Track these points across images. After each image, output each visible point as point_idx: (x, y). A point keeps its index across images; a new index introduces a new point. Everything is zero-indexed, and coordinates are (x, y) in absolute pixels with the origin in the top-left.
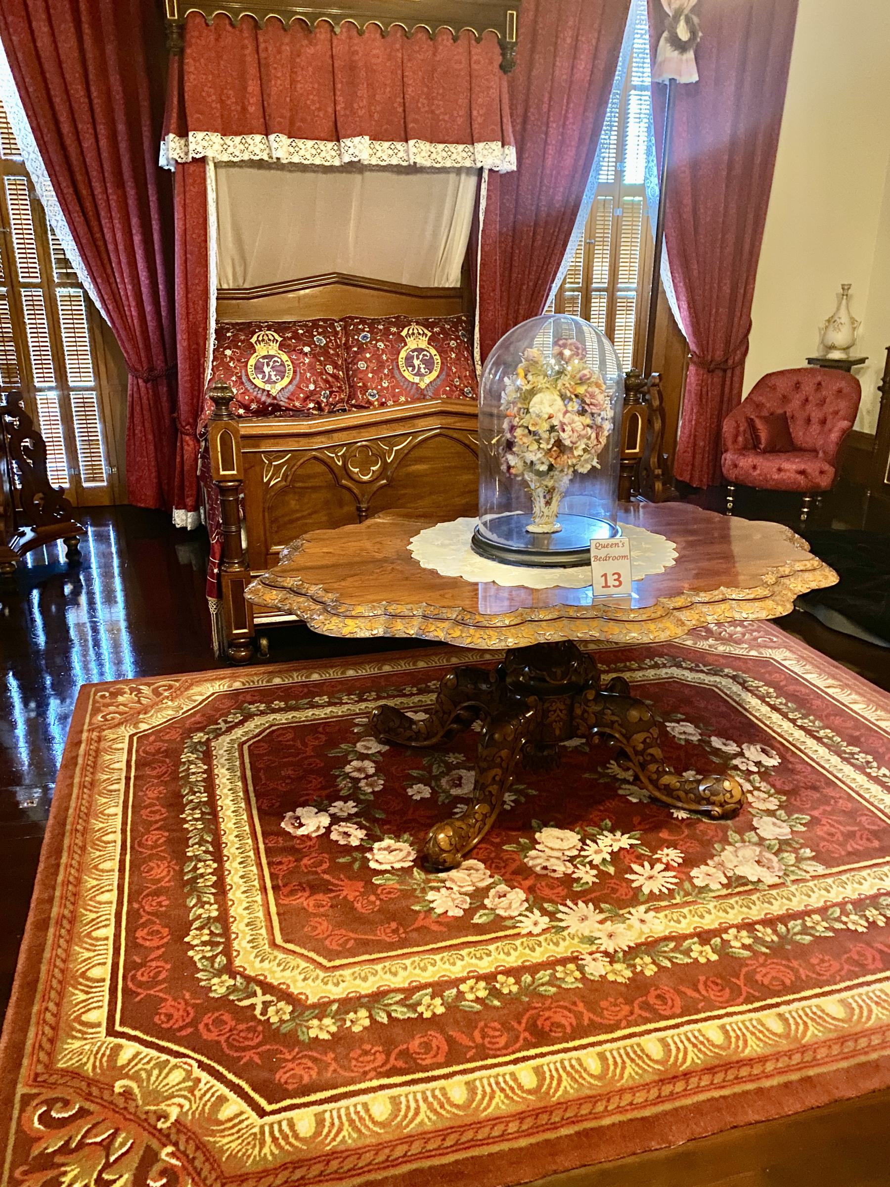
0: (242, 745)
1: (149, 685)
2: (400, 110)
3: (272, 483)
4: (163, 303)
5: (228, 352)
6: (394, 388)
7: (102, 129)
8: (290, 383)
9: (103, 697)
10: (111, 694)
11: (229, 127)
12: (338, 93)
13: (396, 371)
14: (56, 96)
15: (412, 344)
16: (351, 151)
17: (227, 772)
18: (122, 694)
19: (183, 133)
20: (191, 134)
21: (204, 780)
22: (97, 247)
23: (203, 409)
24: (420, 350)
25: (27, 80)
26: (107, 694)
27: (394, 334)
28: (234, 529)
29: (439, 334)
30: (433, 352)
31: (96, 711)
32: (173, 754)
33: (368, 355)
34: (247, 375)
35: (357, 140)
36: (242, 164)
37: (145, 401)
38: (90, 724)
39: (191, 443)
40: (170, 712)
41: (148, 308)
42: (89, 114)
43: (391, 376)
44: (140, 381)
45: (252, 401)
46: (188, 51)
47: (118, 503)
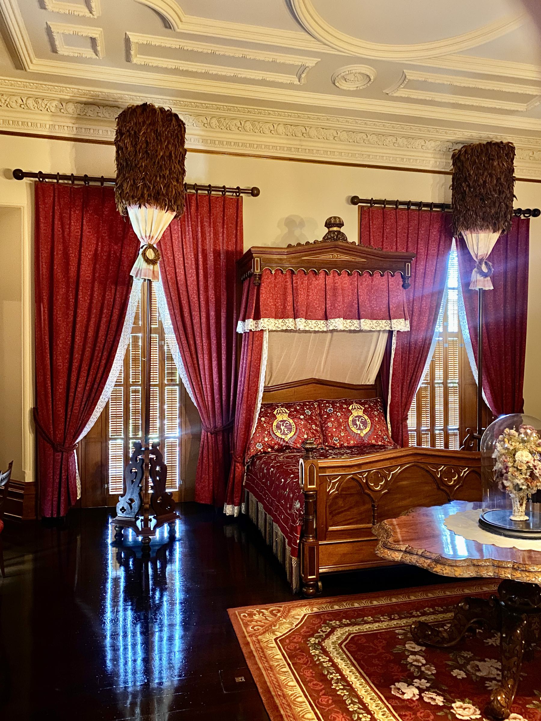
0: (340, 645)
1: (267, 609)
2: (356, 306)
3: (331, 492)
4: (224, 394)
5: (263, 419)
6: (347, 436)
7: (204, 314)
8: (294, 434)
9: (244, 616)
10: (248, 614)
11: (281, 315)
12: (328, 300)
13: (348, 428)
14: (184, 300)
16: (333, 325)
17: (341, 661)
18: (255, 615)
19: (257, 317)
20: (262, 319)
21: (332, 666)
22: (194, 367)
23: (249, 449)
25: (172, 294)
26: (247, 615)
27: (345, 408)
28: (311, 517)
29: (368, 408)
30: (366, 417)
31: (246, 625)
32: (304, 650)
33: (333, 419)
34: (273, 431)
35: (337, 320)
36: (282, 331)
37: (210, 444)
38: (248, 633)
39: (240, 467)
40: (288, 626)
41: (217, 396)
42: (198, 308)
43: (345, 430)
44: (209, 434)
45: (276, 444)
46: (263, 284)
47: (183, 501)
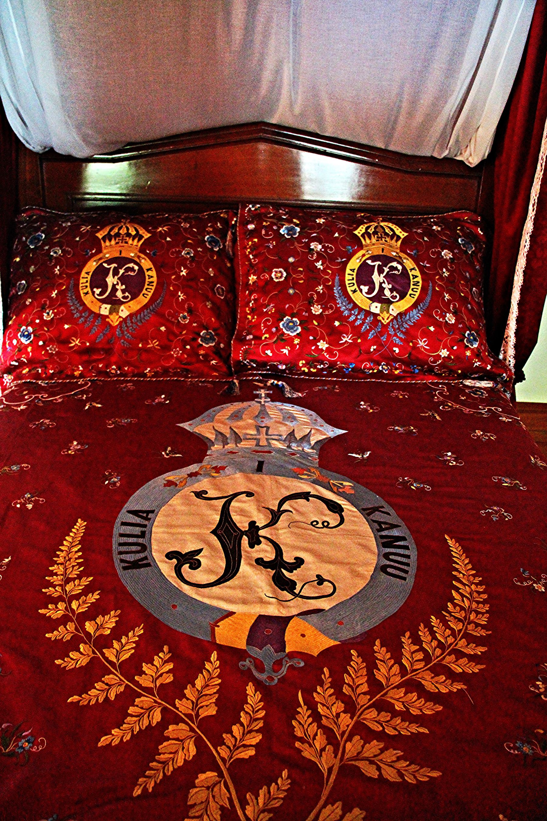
15: (110, 249)
24: (121, 261)
27: (82, 235)
30: (146, 263)
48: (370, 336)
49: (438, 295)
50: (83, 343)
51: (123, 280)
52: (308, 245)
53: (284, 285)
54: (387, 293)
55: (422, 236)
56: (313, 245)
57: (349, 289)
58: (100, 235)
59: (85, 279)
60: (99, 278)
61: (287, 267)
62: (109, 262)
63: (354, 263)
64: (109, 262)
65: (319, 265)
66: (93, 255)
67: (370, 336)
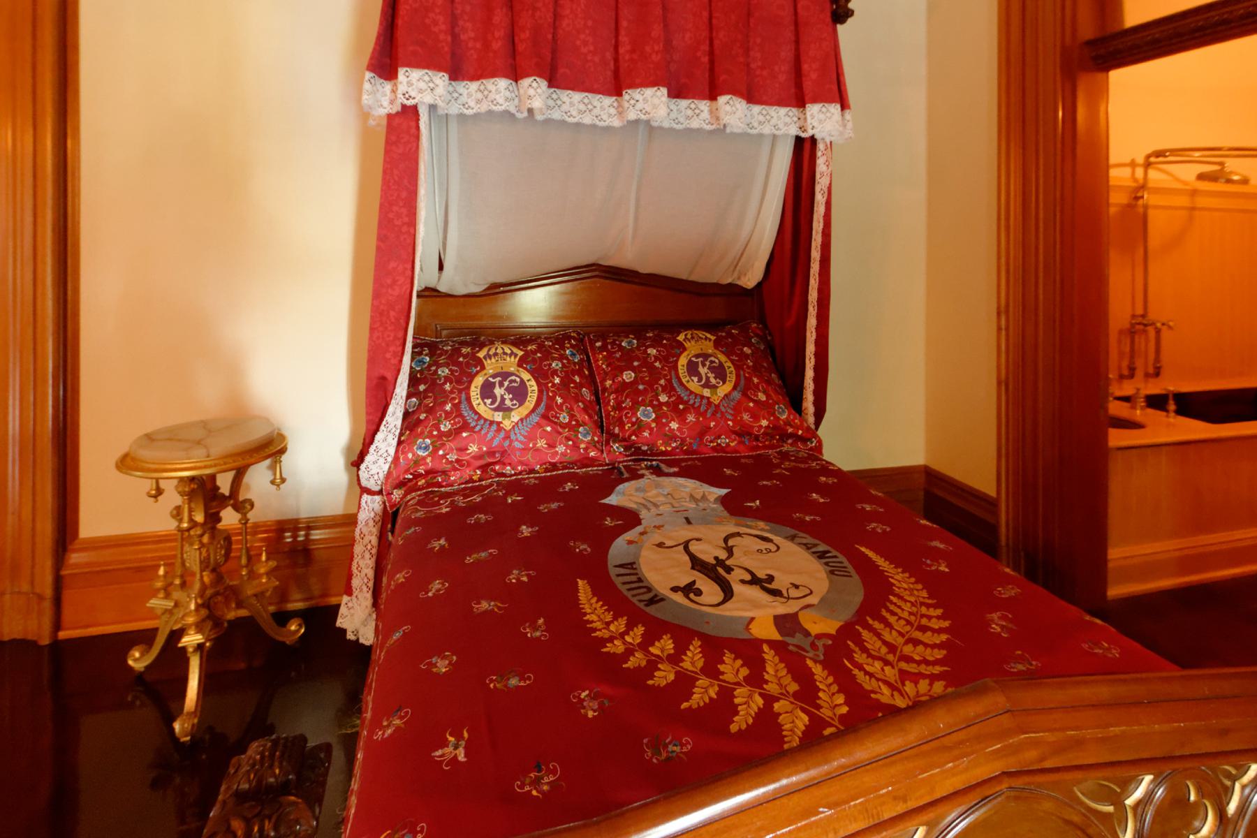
13: (464, 406)
15: (491, 367)
27: (465, 356)
30: (526, 376)
48: (709, 415)
49: (749, 380)
50: (480, 449)
51: (509, 390)
52: (645, 351)
53: (635, 382)
54: (713, 381)
55: (726, 338)
56: (649, 351)
57: (684, 380)
58: (481, 355)
59: (475, 391)
60: (487, 391)
61: (633, 369)
62: (494, 376)
63: (683, 361)
64: (494, 376)
65: (657, 364)
66: (477, 373)
67: (709, 415)
